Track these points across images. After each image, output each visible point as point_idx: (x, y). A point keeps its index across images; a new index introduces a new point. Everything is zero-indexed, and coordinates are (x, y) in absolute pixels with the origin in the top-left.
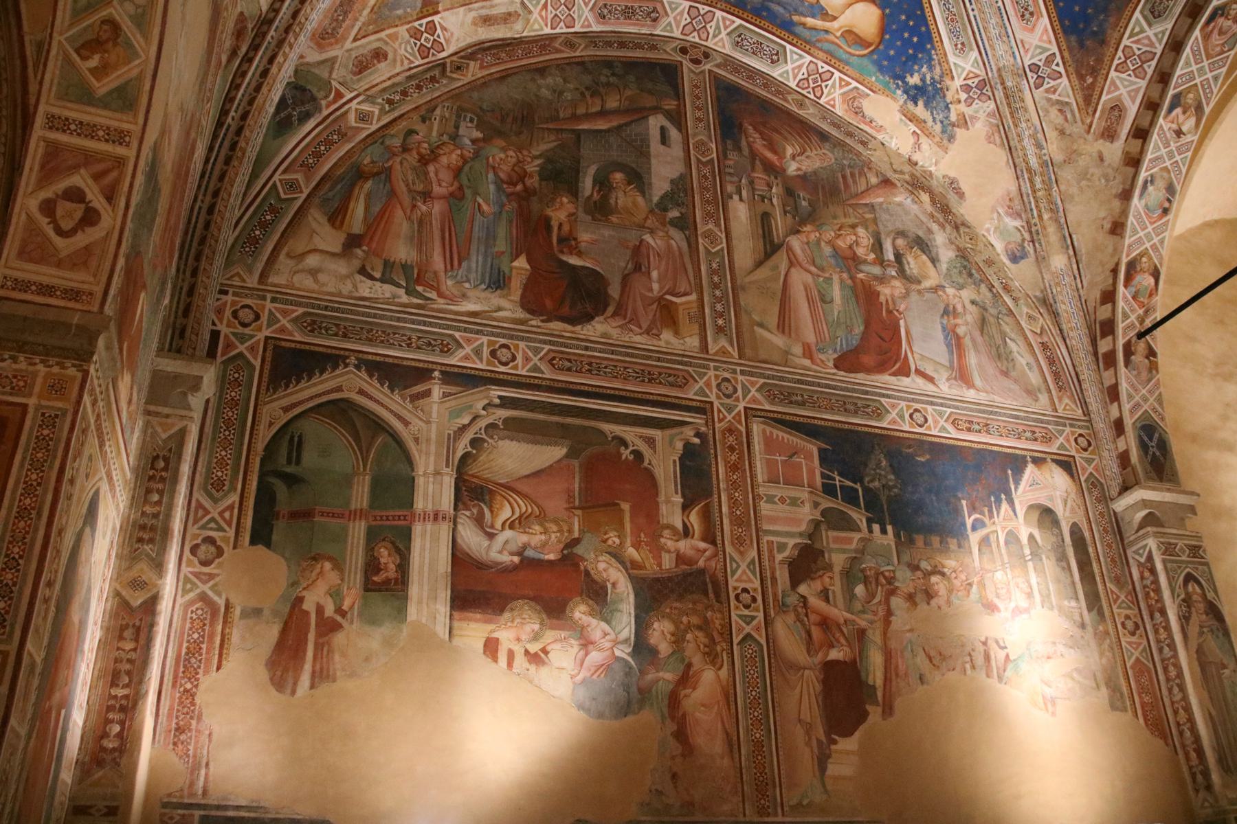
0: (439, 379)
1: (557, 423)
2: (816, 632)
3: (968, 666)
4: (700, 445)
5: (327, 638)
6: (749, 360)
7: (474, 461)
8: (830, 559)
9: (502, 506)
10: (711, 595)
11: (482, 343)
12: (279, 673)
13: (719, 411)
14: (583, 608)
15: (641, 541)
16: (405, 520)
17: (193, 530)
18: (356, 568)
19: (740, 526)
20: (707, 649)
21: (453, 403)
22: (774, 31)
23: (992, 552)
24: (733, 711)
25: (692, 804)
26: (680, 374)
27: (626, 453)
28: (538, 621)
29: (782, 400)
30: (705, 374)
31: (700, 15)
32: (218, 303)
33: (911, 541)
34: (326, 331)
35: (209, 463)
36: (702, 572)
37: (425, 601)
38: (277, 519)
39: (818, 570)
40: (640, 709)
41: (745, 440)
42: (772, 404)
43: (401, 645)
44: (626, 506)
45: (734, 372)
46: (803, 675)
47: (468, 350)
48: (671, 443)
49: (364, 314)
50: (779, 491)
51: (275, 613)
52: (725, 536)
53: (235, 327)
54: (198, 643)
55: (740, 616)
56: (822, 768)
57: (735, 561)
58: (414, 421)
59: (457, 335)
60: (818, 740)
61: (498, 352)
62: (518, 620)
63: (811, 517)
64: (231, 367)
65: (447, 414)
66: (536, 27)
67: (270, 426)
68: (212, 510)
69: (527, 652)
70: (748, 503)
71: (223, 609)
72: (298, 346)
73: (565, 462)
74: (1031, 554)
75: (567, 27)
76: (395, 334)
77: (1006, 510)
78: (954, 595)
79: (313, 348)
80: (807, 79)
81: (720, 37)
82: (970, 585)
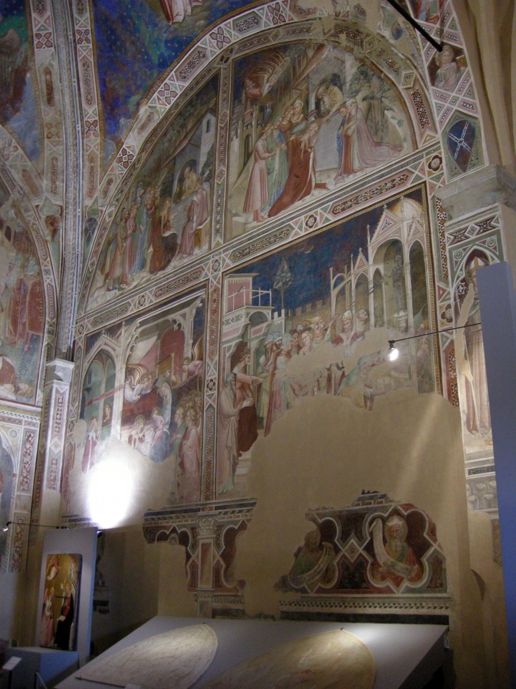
2: (238, 393)
3: (316, 389)
8: (250, 346)
10: (198, 388)
23: (345, 298)
31: (217, 34)
50: (231, 316)
56: (234, 470)
60: (233, 455)
63: (245, 323)
66: (163, 110)
74: (374, 287)
75: (175, 97)
77: (361, 260)
78: (314, 341)
82: (326, 330)
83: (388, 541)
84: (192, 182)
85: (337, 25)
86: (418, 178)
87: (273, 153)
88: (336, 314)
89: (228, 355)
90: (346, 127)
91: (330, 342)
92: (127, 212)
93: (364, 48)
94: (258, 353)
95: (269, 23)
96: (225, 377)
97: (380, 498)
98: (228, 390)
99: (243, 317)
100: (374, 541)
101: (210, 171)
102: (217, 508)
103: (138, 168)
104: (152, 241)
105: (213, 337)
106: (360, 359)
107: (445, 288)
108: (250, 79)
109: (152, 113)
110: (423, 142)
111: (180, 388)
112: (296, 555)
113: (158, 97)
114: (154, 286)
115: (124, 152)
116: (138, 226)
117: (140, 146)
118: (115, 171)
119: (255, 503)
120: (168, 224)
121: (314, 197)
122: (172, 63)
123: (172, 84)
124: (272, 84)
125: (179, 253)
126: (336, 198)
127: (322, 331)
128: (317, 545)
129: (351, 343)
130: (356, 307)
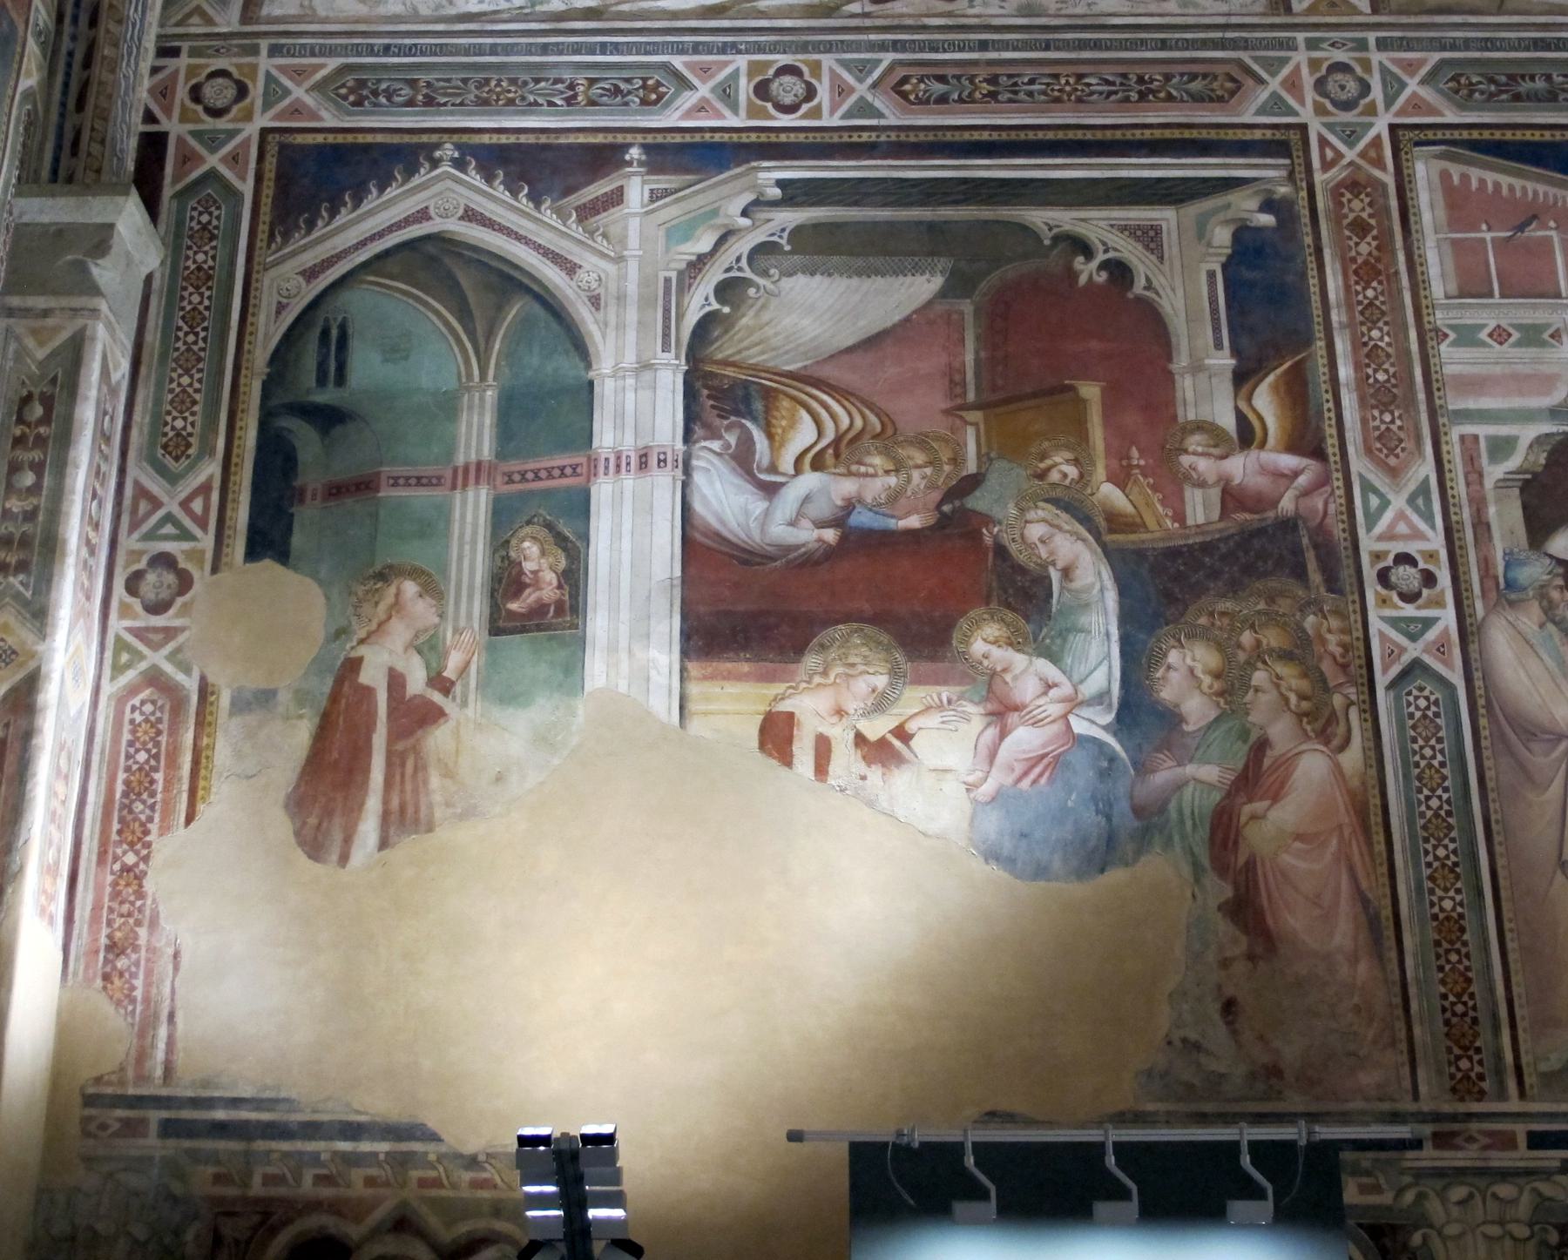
0: (641, 163)
1: (919, 223)
4: (1274, 229)
5: (410, 742)
6: (1400, 12)
7: (726, 331)
9: (793, 423)
10: (1315, 577)
11: (737, 70)
12: (313, 821)
13: (1323, 143)
14: (992, 630)
15: (1130, 466)
16: (575, 473)
17: (129, 542)
18: (471, 587)
19: (1385, 407)
20: (1305, 705)
21: (674, 211)
24: (1380, 847)
25: (1274, 1071)
26: (1219, 69)
27: (1088, 271)
28: (883, 668)
29: (1492, 95)
30: (1284, 61)
32: (160, 76)
34: (389, 99)
35: (158, 402)
36: (1288, 525)
37: (624, 643)
38: (302, 501)
40: (1138, 853)
41: (1394, 203)
42: (1462, 107)
43: (575, 741)
44: (1090, 391)
45: (1362, 45)
47: (704, 90)
48: (1201, 232)
49: (467, 51)
50: (1486, 315)
51: (301, 697)
52: (1349, 435)
53: (199, 121)
54: (147, 772)
55: (1394, 622)
57: (1376, 491)
58: (587, 260)
59: (678, 62)
61: (774, 86)
62: (838, 669)
64: (193, 203)
65: (662, 233)
67: (278, 312)
68: (165, 499)
69: (860, 739)
70: (1408, 352)
71: (194, 698)
72: (331, 138)
73: (940, 308)
76: (537, 81)
79: (361, 139)
89: (1494, 472)
98: (1530, 619)
102: (1538, 1141)
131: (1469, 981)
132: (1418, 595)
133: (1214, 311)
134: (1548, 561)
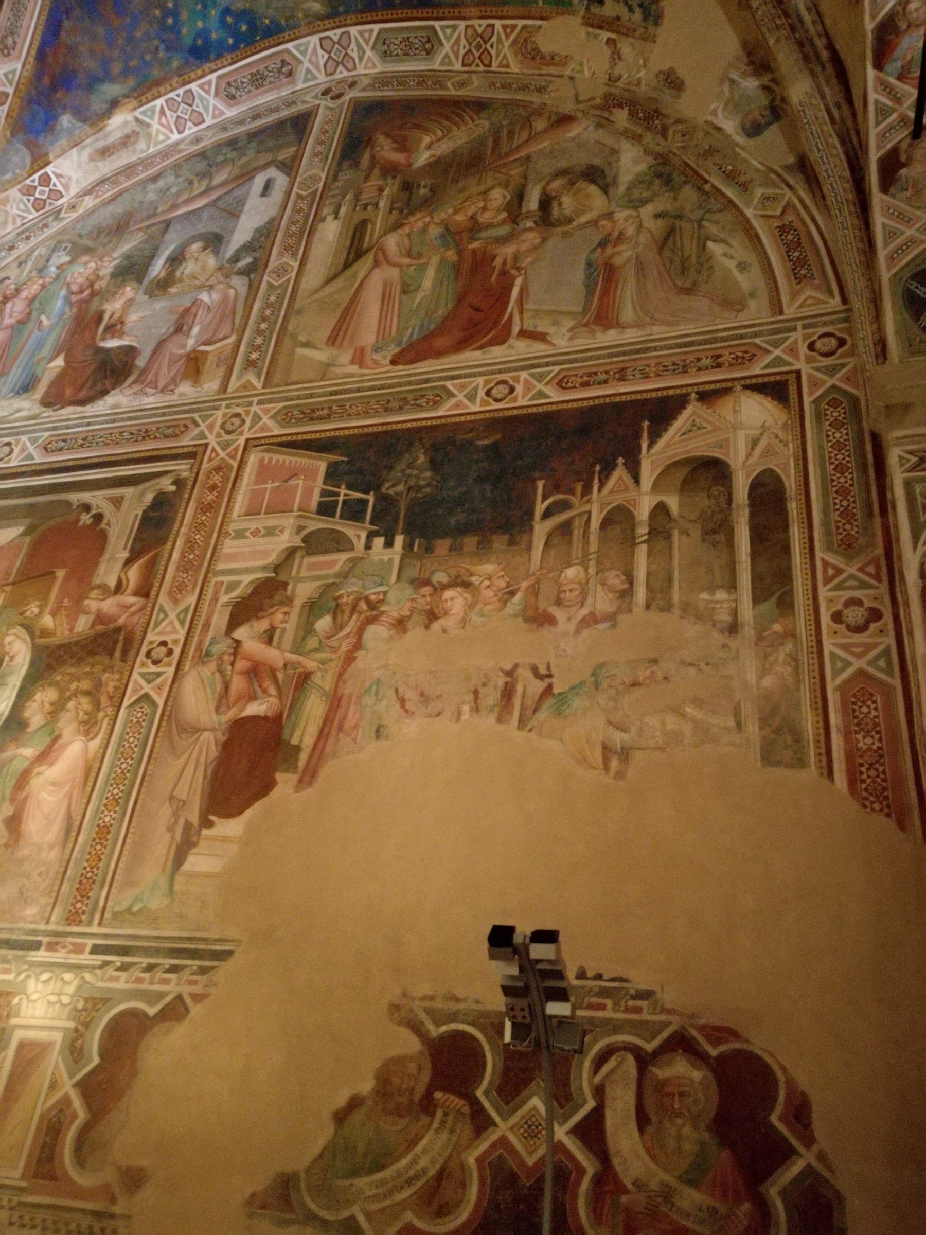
2: (238, 684)
3: (466, 708)
8: (293, 590)
10: (118, 654)
19: (186, 571)
22: (415, 14)
23: (570, 543)
24: (89, 789)
31: (334, 43)
33: (429, 549)
39: (272, 606)
41: (233, 475)
42: (284, 427)
46: (198, 739)
56: (180, 859)
66: (161, 137)
74: (649, 533)
75: (196, 125)
77: (620, 478)
80: (470, 51)
81: (366, 57)
82: (512, 593)
83: (654, 1119)
84: (203, 269)
85: (607, 96)
86: (778, 361)
87: (422, 261)
88: (541, 568)
89: (224, 598)
90: (609, 251)
91: (520, 620)
92: (13, 287)
93: (670, 138)
94: (313, 608)
95: (453, 59)
96: (207, 643)
97: (634, 998)
98: (208, 670)
99: (287, 533)
100: (608, 1113)
101: (255, 259)
102: (96, 950)
103: (64, 219)
104: (66, 348)
105: (191, 557)
106: (601, 666)
107: (842, 566)
108: (387, 135)
109: (135, 134)
110: (797, 304)
111: (62, 646)
112: (340, 1117)
113: (162, 107)
114: (48, 430)
115: (46, 180)
116: (34, 314)
117: (85, 185)
118: (9, 206)
119: (229, 953)
120: (119, 327)
121: (513, 352)
122: (219, 56)
123: (201, 98)
124: (439, 153)
125: (134, 382)
126: (571, 361)
127: (500, 594)
128: (417, 1097)
129: (578, 631)
130: (599, 562)
131: (100, 860)
132: (160, 661)
133: (131, 532)
134: (230, 641)
